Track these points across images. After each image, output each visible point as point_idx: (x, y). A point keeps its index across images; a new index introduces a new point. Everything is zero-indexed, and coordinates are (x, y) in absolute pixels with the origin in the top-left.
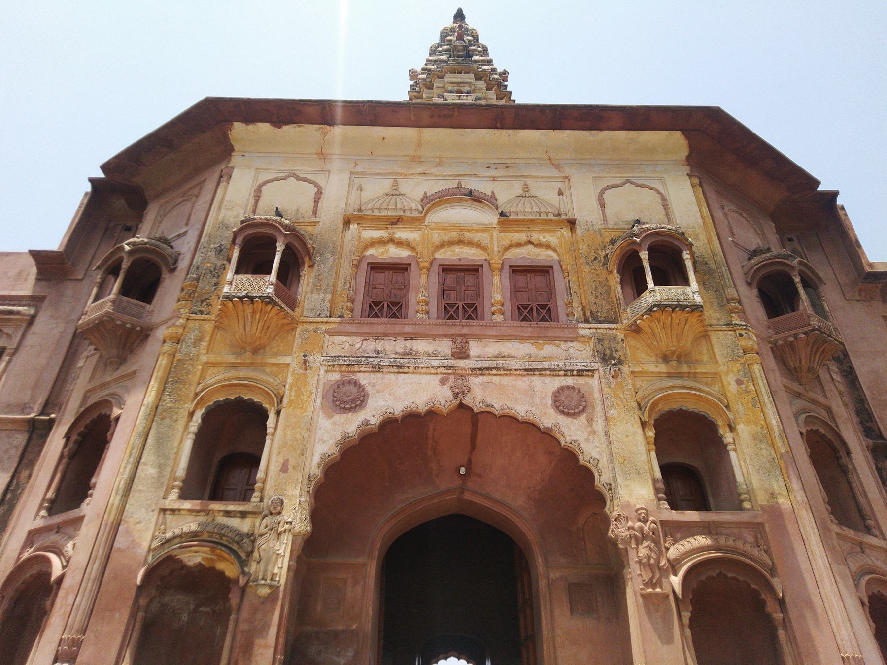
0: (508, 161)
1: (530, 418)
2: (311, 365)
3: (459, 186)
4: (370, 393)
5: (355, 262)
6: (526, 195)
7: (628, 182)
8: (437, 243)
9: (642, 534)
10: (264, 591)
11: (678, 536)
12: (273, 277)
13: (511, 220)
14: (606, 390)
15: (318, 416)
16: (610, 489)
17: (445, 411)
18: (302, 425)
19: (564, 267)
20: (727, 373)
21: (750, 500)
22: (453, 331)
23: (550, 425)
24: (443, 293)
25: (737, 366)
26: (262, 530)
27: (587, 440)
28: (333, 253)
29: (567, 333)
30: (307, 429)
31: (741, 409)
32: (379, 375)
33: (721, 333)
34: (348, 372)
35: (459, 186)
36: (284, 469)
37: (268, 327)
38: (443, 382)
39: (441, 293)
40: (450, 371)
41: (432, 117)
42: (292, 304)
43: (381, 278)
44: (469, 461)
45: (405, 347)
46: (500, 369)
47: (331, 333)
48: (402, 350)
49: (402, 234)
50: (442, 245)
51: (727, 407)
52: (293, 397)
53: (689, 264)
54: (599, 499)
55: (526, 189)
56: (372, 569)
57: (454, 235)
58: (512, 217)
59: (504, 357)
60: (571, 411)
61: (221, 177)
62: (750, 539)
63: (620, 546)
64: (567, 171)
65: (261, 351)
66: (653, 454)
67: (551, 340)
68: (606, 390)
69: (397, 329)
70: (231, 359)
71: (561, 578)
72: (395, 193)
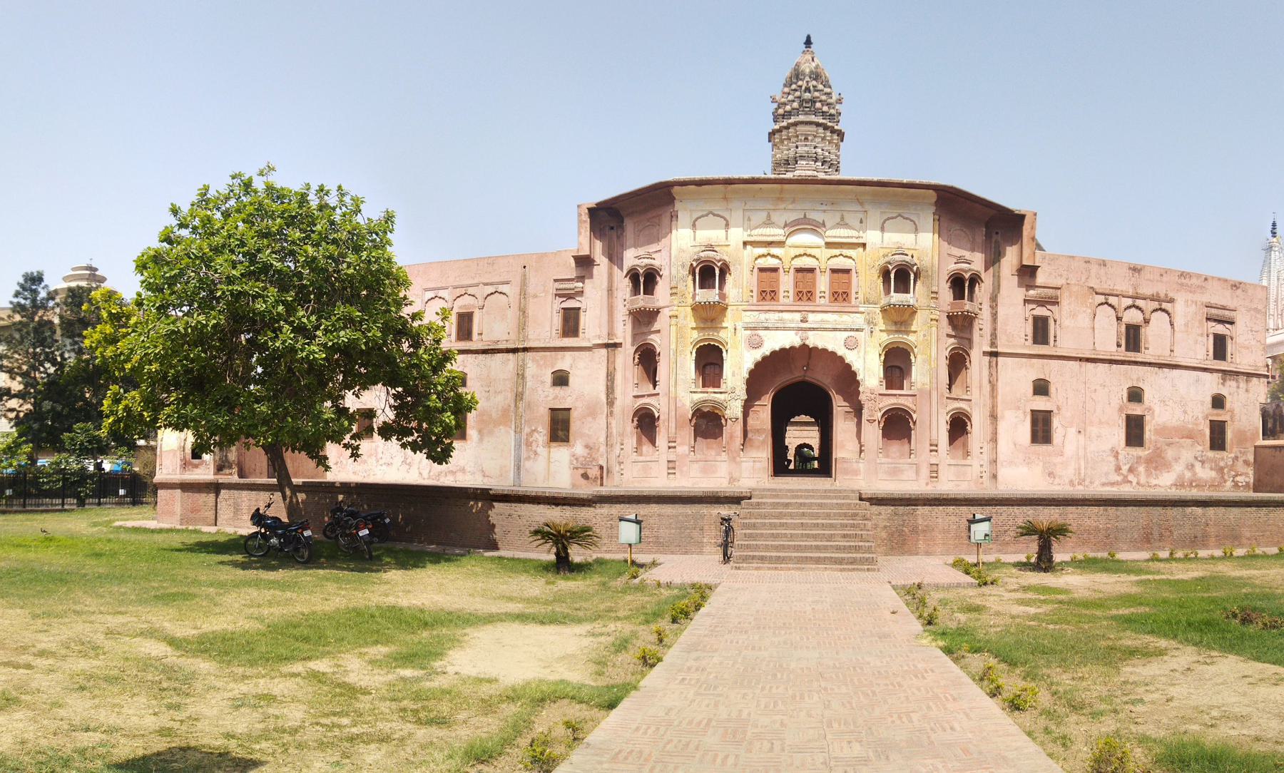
12: (717, 290)
24: (796, 286)
49: (774, 251)
54: (858, 383)
57: (801, 251)
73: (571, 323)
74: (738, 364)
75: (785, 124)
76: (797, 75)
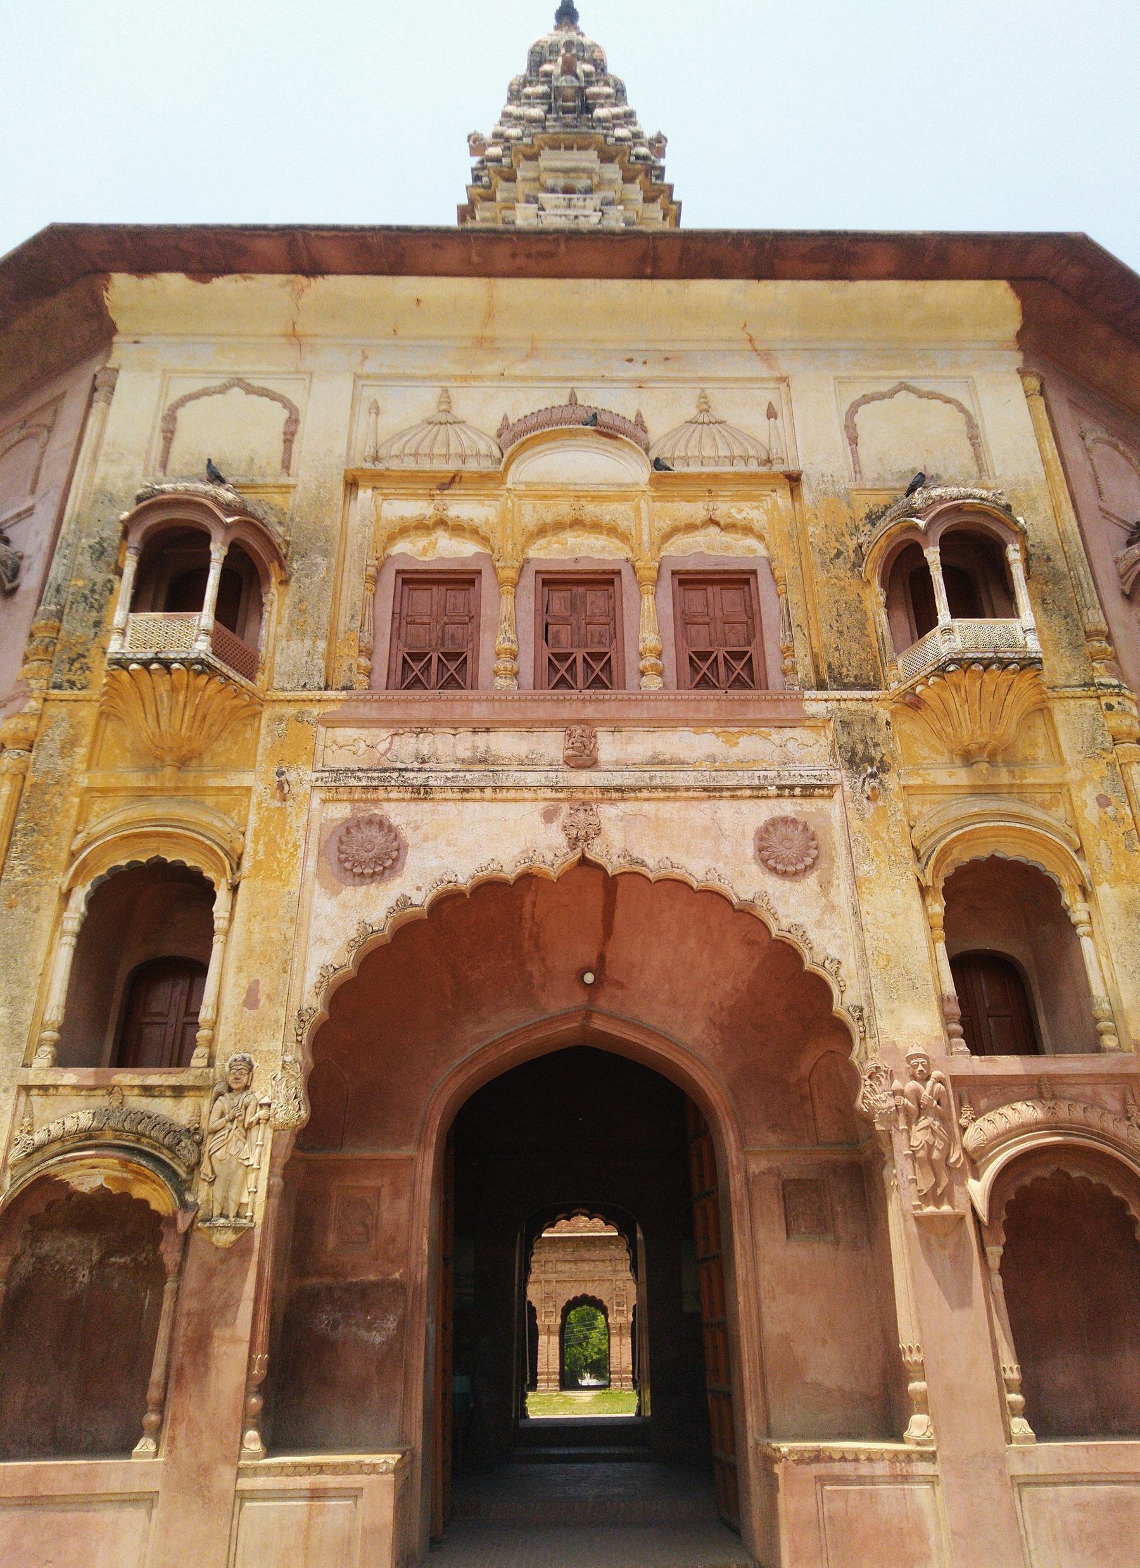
0: (668, 346)
1: (715, 884)
2: (294, 791)
3: (573, 402)
4: (410, 842)
5: (372, 571)
6: (705, 418)
7: (903, 387)
8: (532, 527)
9: (919, 1104)
10: (225, 1239)
11: (983, 1103)
12: (206, 617)
13: (675, 477)
14: (856, 824)
15: (312, 892)
16: (860, 1018)
17: (553, 874)
18: (281, 912)
19: (777, 574)
20: (1081, 784)
21: (1115, 1032)
22: (565, 712)
23: (750, 897)
24: (545, 633)
25: (1100, 769)
26: (215, 1122)
27: (819, 924)
28: (325, 553)
29: (783, 711)
30: (292, 920)
31: (1105, 856)
32: (426, 805)
33: (1072, 702)
34: (365, 801)
35: (573, 402)
36: (251, 1000)
37: (204, 717)
38: (549, 816)
39: (541, 632)
40: (561, 795)
41: (514, 256)
42: (249, 665)
43: (424, 600)
44: (602, 957)
45: (475, 748)
46: (656, 788)
47: (330, 722)
48: (467, 754)
49: (462, 509)
50: (542, 531)
51: (1079, 851)
52: (261, 856)
53: (1018, 572)
55: (704, 405)
56: (426, 1166)
57: (563, 509)
58: (679, 468)
59: (663, 762)
60: (791, 869)
61: (94, 389)
62: (1114, 1104)
63: (878, 1127)
64: (786, 366)
65: (194, 762)
66: (941, 947)
67: (754, 725)
68: (856, 824)
69: (458, 711)
70: (136, 780)
71: (770, 1170)
74: (281, 953)
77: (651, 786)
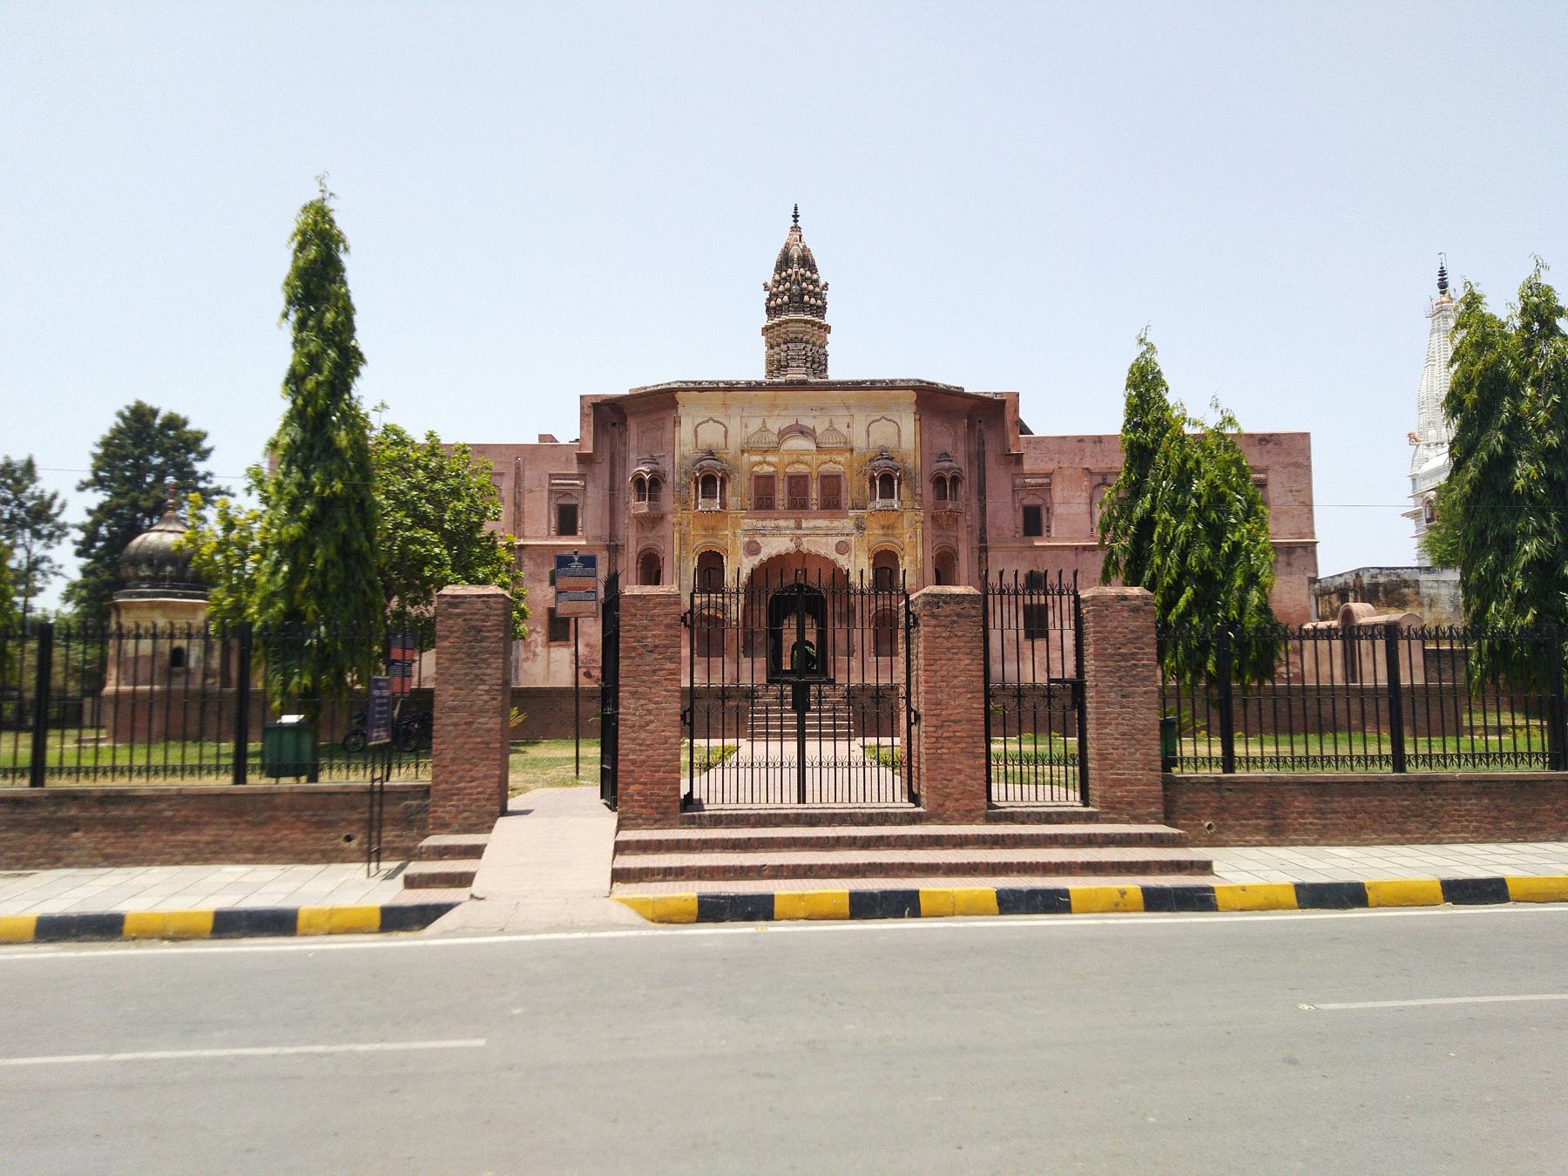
6: (831, 429)
49: (770, 458)
72: (764, 429)
73: (567, 521)
74: (739, 567)
75: (776, 320)
76: (785, 261)
77: (815, 532)
